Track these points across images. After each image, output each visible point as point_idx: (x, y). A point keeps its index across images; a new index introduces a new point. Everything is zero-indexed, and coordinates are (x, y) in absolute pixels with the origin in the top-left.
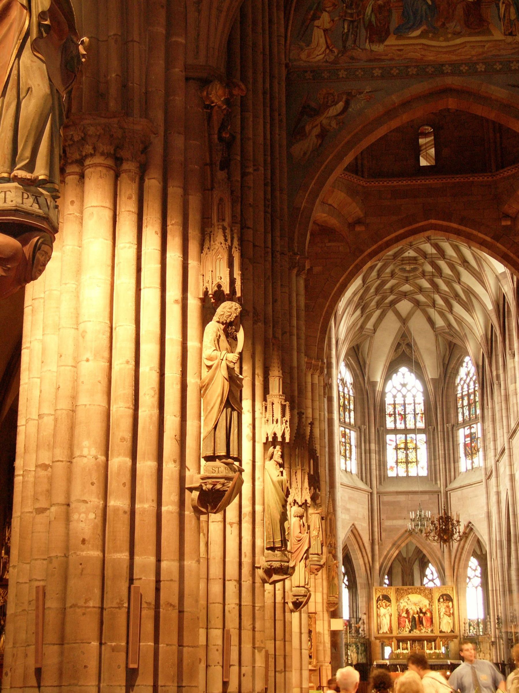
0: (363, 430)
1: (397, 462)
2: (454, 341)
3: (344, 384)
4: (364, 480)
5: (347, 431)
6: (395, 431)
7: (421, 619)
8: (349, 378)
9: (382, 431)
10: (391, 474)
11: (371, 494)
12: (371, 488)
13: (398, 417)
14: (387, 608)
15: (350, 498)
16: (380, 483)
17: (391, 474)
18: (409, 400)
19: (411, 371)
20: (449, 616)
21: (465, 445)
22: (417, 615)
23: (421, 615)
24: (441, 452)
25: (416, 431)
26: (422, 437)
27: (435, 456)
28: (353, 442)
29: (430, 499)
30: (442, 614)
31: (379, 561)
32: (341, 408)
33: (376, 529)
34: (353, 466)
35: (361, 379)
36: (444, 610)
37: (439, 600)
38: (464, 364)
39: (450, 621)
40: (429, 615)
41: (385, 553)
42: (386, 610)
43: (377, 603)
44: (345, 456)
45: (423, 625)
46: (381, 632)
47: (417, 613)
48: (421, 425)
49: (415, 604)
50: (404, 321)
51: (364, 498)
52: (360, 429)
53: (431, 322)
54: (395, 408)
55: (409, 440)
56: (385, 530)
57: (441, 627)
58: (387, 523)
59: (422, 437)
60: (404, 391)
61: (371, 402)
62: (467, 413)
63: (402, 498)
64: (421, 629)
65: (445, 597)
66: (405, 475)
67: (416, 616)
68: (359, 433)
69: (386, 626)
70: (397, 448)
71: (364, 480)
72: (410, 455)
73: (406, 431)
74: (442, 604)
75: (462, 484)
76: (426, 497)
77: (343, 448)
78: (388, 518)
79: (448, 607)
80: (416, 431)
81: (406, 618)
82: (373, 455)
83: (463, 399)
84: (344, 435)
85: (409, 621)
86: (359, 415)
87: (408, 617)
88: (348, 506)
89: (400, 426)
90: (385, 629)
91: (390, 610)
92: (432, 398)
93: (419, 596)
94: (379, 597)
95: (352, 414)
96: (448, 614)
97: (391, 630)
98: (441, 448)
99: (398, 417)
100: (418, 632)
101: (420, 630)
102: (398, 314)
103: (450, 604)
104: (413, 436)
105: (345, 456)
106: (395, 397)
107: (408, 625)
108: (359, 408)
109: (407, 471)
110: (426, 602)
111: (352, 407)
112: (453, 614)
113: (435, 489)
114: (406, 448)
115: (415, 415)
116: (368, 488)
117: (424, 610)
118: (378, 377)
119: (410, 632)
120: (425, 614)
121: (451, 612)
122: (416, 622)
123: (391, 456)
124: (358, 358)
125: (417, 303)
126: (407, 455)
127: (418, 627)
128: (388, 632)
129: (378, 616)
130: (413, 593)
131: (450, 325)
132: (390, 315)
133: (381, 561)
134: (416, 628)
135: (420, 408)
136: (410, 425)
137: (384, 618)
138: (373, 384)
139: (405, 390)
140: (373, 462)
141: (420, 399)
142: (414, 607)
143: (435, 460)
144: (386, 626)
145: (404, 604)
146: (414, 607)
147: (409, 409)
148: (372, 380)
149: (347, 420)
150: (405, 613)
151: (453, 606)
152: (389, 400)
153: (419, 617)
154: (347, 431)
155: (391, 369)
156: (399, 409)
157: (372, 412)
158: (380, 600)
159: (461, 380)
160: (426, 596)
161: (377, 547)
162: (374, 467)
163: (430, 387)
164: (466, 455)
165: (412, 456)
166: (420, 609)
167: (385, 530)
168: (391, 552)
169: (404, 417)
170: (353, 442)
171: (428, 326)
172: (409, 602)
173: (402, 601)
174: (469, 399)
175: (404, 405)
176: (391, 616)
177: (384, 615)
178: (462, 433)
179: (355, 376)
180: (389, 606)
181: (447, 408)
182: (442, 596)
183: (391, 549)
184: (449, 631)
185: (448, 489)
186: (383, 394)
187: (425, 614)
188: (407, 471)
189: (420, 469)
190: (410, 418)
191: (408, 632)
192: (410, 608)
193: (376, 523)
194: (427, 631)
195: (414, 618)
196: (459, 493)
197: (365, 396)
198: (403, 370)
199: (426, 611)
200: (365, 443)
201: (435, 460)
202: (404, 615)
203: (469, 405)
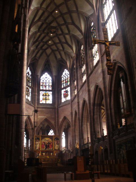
1: (43, 99)
2: (62, 64)
3: (29, 74)
5: (29, 88)
6: (43, 90)
9: (39, 90)
10: (41, 102)
15: (28, 107)
16: (38, 105)
17: (41, 102)
18: (47, 81)
19: (49, 74)
20: (58, 144)
21: (64, 94)
24: (56, 97)
25: (49, 91)
26: (51, 92)
28: (30, 92)
34: (29, 98)
37: (54, 140)
38: (64, 72)
40: (51, 144)
44: (28, 95)
45: (49, 147)
47: (48, 143)
48: (50, 89)
49: (47, 141)
53: (56, 57)
54: (43, 84)
55: (47, 93)
56: (38, 119)
59: (51, 92)
60: (46, 79)
61: (36, 80)
62: (65, 85)
63: (44, 109)
66: (45, 103)
67: (47, 144)
72: (47, 97)
73: (46, 91)
75: (63, 105)
76: (51, 110)
78: (40, 115)
79: (57, 142)
80: (49, 91)
82: (36, 96)
83: (63, 81)
84: (28, 89)
88: (28, 110)
89: (44, 89)
90: (37, 148)
92: (54, 80)
95: (30, 84)
97: (39, 149)
99: (44, 87)
102: (47, 54)
104: (48, 92)
106: (43, 81)
109: (46, 102)
110: (50, 140)
111: (30, 81)
113: (54, 107)
115: (49, 86)
117: (50, 143)
118: (39, 74)
119: (45, 149)
120: (50, 144)
122: (47, 146)
123: (41, 97)
124: (33, 66)
125: (53, 51)
129: (36, 144)
131: (62, 57)
132: (44, 55)
135: (51, 84)
136: (47, 89)
138: (38, 76)
139: (46, 79)
140: (36, 98)
141: (51, 81)
142: (47, 142)
145: (43, 140)
146: (47, 142)
147: (47, 84)
149: (29, 85)
152: (41, 81)
153: (48, 145)
154: (29, 88)
156: (44, 84)
157: (37, 84)
159: (63, 76)
160: (51, 138)
162: (36, 100)
163: (54, 78)
164: (64, 97)
165: (47, 98)
168: (40, 126)
169: (46, 86)
170: (30, 92)
171: (55, 59)
174: (66, 81)
175: (46, 83)
176: (39, 144)
177: (37, 144)
178: (63, 91)
179: (32, 72)
186: (40, 80)
187: (50, 144)
188: (46, 102)
189: (50, 101)
193: (36, 116)
196: (62, 108)
198: (46, 73)
202: (44, 144)
203: (66, 82)
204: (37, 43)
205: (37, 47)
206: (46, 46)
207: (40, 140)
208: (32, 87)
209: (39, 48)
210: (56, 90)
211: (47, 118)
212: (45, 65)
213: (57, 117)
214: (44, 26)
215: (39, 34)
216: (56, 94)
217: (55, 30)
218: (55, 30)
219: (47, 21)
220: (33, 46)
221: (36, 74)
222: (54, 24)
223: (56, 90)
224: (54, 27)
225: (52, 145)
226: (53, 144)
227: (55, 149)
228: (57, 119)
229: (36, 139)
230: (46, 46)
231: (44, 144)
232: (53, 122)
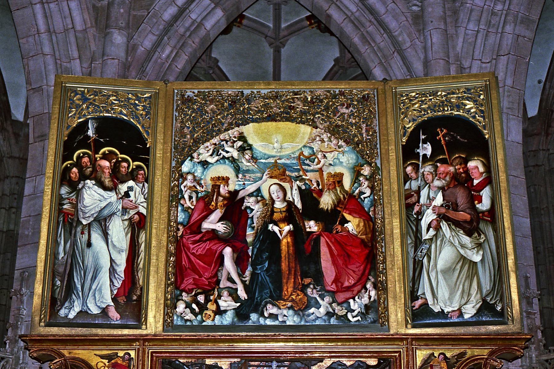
7: (308, 247)
14: (123, 188)
22: (287, 228)
23: (312, 226)
30: (429, 217)
36: (439, 200)
37: (409, 152)
39: (477, 258)
40: (353, 225)
42: (112, 197)
43: (67, 156)
45: (318, 278)
46: (72, 312)
47: (291, 214)
49: (280, 172)
57: (425, 288)
64: (311, 303)
65: (441, 134)
69: (104, 277)
74: (428, 169)
79: (462, 180)
81: (225, 241)
87: (235, 239)
91: (138, 196)
93: (305, 130)
94: (83, 126)
96: (464, 216)
101: (301, 308)
103: (475, 165)
112: (492, 215)
117: (327, 201)
119: (242, 314)
120: (331, 219)
121: (485, 205)
127: (288, 288)
128: (114, 314)
129: (68, 221)
130: (272, 118)
134: (277, 297)
137: (96, 238)
142: (269, 186)
144: (104, 277)
145: (209, 168)
146: (269, 186)
150: (217, 215)
151: (488, 181)
153: (298, 234)
158: (85, 143)
160: (335, 131)
166: (305, 194)
172: (245, 164)
173: (204, 152)
176: (138, 225)
177: (102, 221)
180: (132, 175)
182: (428, 128)
184: (469, 312)
187: (331, 219)
191: (228, 319)
192: (251, 188)
194: (340, 311)
195: (268, 240)
199: (338, 203)
202: (213, 223)
207: (160, 152)
225: (374, 235)
226: (394, 226)
229: (75, 139)
231: (213, 223)
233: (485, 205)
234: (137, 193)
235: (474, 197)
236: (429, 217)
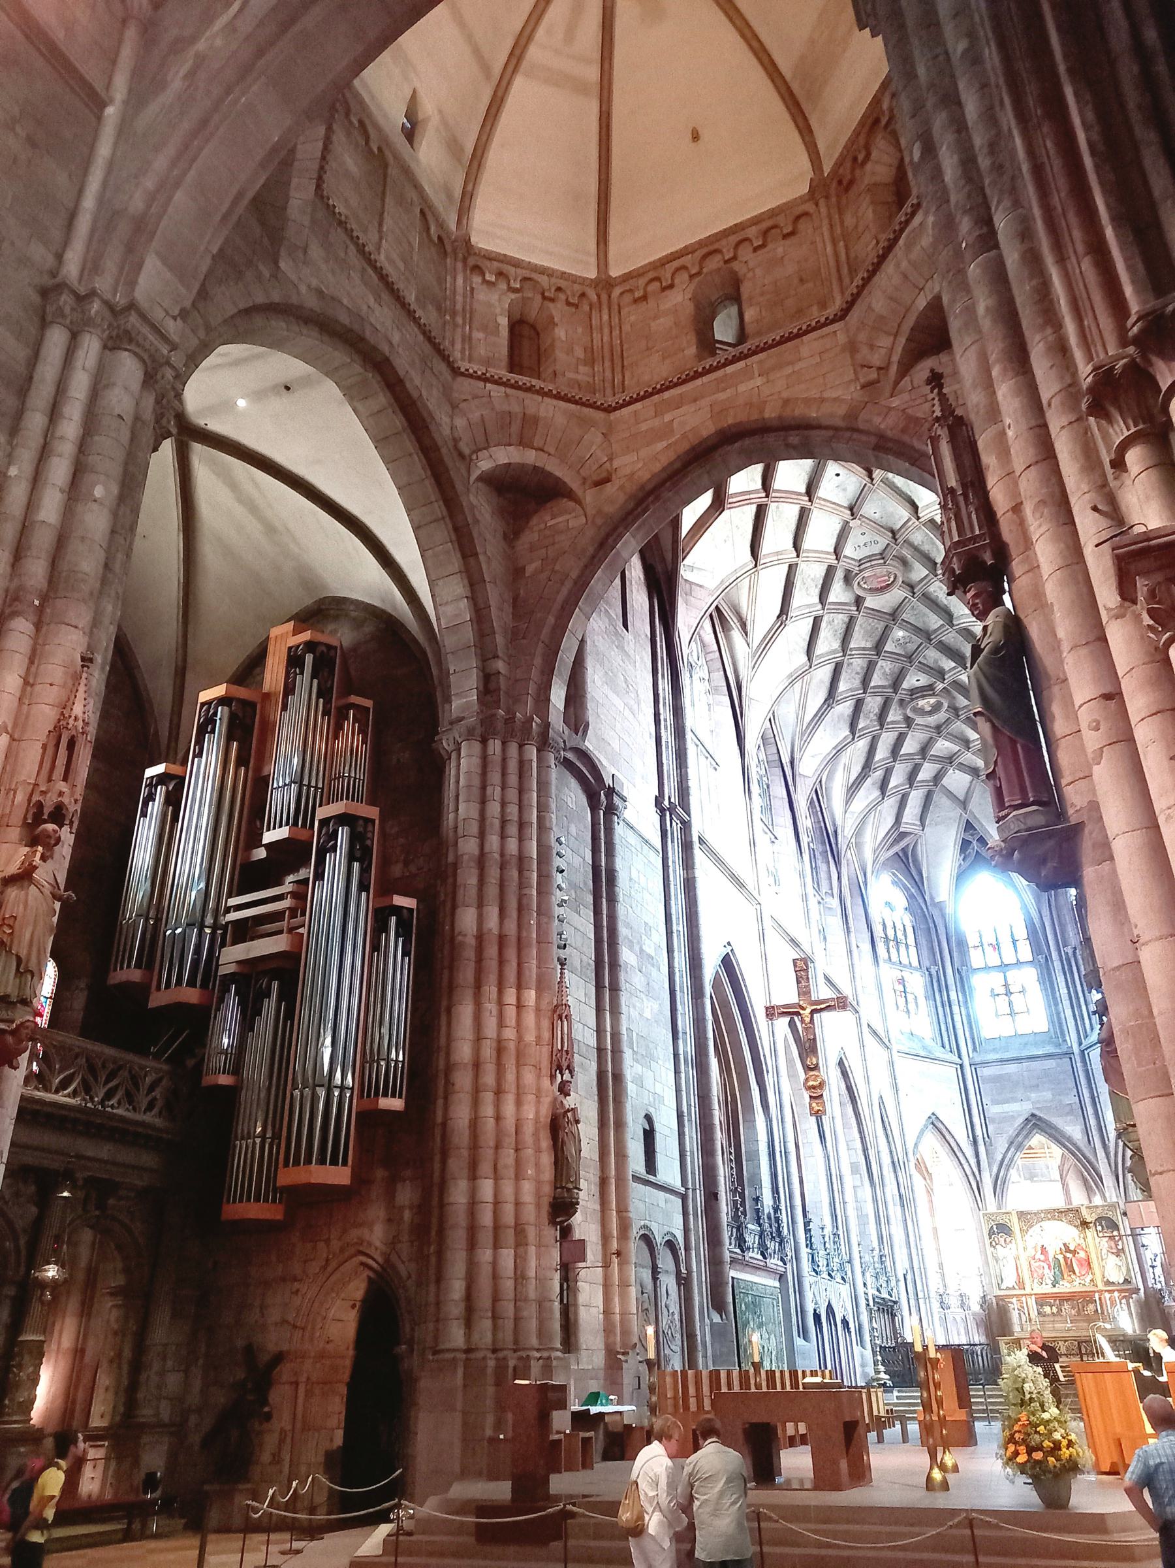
0: (933, 970)
4: (947, 1046)
6: (987, 968)
8: (900, 900)
11: (961, 1065)
12: (960, 1057)
13: (989, 950)
16: (975, 1049)
24: (1064, 991)
27: (1054, 998)
29: (1058, 1065)
31: (991, 1172)
32: (891, 944)
33: (976, 1120)
35: (921, 901)
40: (1082, 1254)
41: (999, 1158)
50: (964, 804)
51: (951, 1072)
52: (930, 975)
56: (993, 1121)
57: (1106, 1274)
58: (993, 1110)
61: (942, 931)
63: (1012, 1068)
67: (1061, 1257)
68: (928, 979)
70: (994, 995)
71: (947, 1046)
73: (1003, 967)
76: (1051, 1064)
77: (902, 1001)
78: (995, 1102)
80: (1019, 963)
82: (955, 1009)
84: (902, 981)
85: (1049, 1267)
86: (925, 952)
89: (994, 960)
90: (1010, 1281)
95: (913, 950)
98: (1062, 984)
100: (1068, 1285)
103: (1115, 1233)
105: (908, 1011)
107: (1049, 1274)
108: (923, 942)
113: (1064, 1049)
114: (1008, 993)
115: (1014, 942)
116: (956, 1059)
117: (1072, 1248)
120: (1074, 1252)
121: (1120, 1247)
126: (1010, 1003)
132: (939, 798)
133: (995, 1170)
136: (1009, 958)
138: (940, 906)
140: (957, 1018)
143: (1056, 1005)
148: (937, 900)
149: (905, 961)
155: (961, 876)
161: (982, 1149)
167: (993, 1121)
169: (997, 947)
176: (1017, 1258)
179: (911, 897)
181: (1060, 924)
183: (1008, 1149)
185: (1083, 1047)
190: (1007, 947)
197: (932, 925)
200: (940, 991)
201: (1056, 1005)
202: (1039, 1256)
204: (879, 774)
205: (883, 786)
206: (927, 771)
208: (926, 963)
209: (895, 787)
210: (1055, 955)
211: (1037, 1113)
212: (965, 845)
213: (1088, 1100)
214: (873, 704)
215: (862, 745)
216: (1061, 979)
217: (932, 701)
218: (932, 701)
219: (876, 680)
220: (862, 792)
221: (932, 898)
222: (915, 679)
223: (1055, 955)
224: (922, 689)
226: (1093, 1256)
227: (1108, 1283)
228: (1090, 1110)
229: (991, 1233)
230: (927, 771)
232: (1075, 1131)
233: (1120, 1247)
234: (1013, 1245)
235: (1117, 1245)
236: (1104, 1251)
